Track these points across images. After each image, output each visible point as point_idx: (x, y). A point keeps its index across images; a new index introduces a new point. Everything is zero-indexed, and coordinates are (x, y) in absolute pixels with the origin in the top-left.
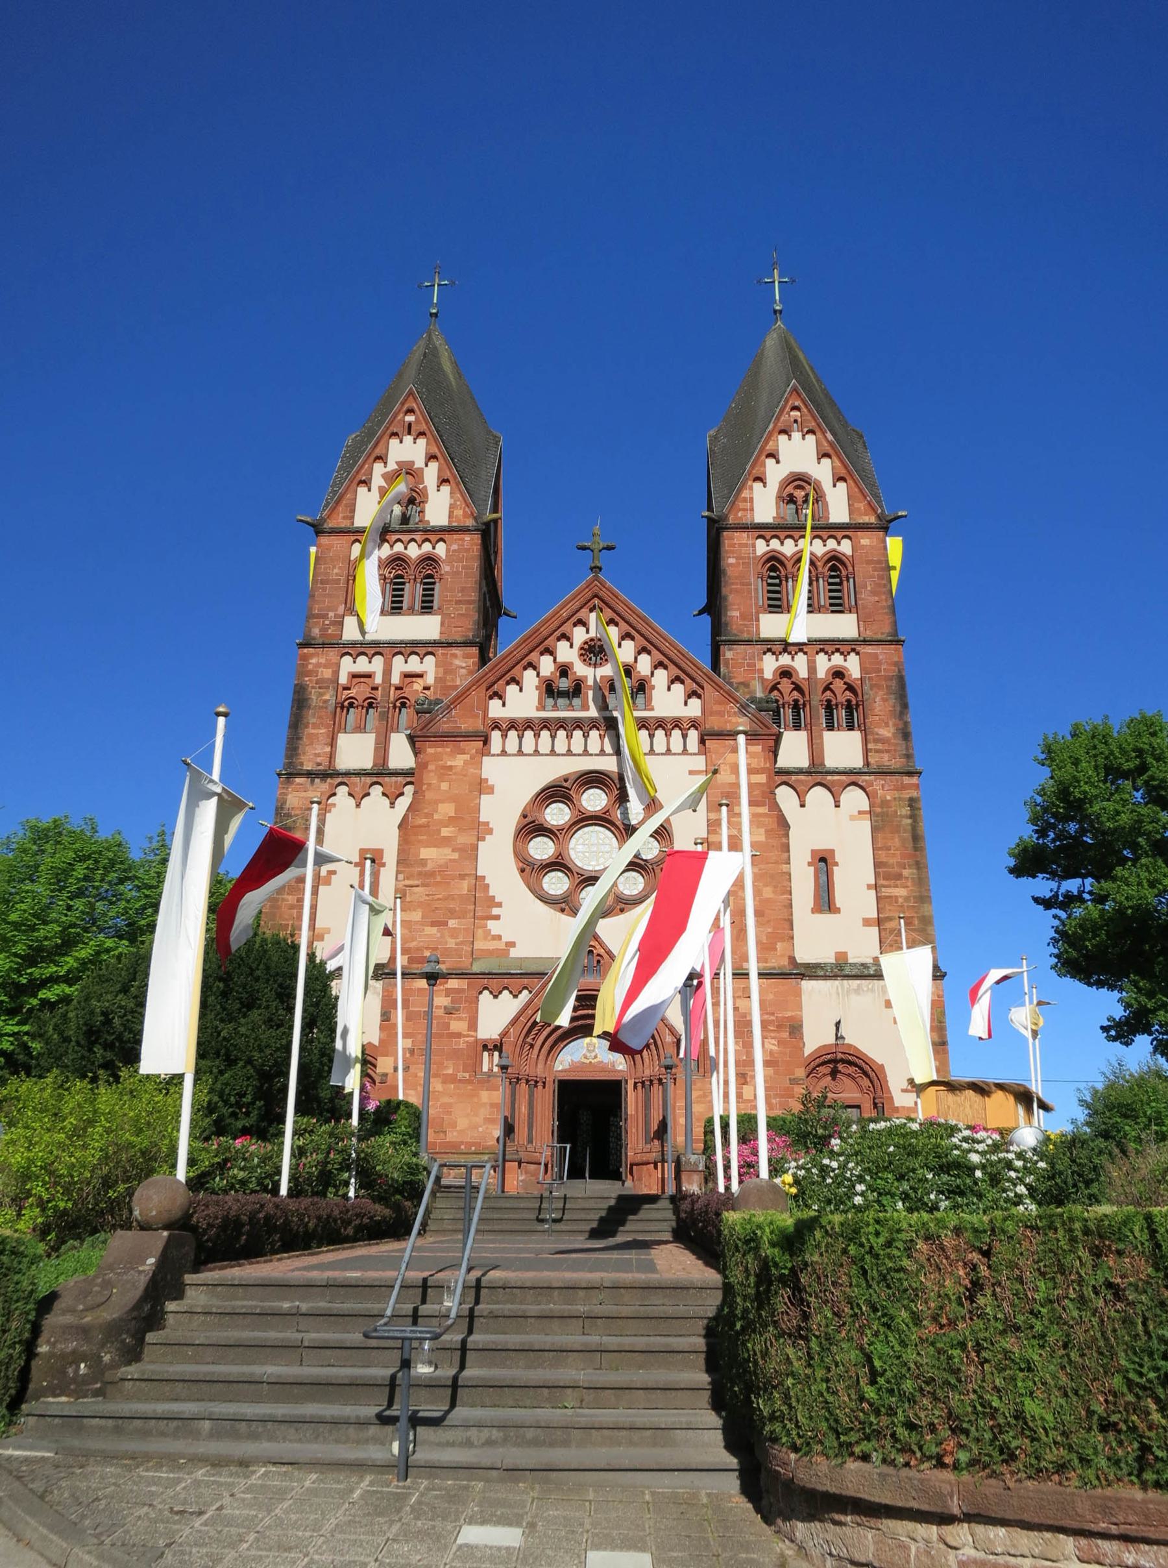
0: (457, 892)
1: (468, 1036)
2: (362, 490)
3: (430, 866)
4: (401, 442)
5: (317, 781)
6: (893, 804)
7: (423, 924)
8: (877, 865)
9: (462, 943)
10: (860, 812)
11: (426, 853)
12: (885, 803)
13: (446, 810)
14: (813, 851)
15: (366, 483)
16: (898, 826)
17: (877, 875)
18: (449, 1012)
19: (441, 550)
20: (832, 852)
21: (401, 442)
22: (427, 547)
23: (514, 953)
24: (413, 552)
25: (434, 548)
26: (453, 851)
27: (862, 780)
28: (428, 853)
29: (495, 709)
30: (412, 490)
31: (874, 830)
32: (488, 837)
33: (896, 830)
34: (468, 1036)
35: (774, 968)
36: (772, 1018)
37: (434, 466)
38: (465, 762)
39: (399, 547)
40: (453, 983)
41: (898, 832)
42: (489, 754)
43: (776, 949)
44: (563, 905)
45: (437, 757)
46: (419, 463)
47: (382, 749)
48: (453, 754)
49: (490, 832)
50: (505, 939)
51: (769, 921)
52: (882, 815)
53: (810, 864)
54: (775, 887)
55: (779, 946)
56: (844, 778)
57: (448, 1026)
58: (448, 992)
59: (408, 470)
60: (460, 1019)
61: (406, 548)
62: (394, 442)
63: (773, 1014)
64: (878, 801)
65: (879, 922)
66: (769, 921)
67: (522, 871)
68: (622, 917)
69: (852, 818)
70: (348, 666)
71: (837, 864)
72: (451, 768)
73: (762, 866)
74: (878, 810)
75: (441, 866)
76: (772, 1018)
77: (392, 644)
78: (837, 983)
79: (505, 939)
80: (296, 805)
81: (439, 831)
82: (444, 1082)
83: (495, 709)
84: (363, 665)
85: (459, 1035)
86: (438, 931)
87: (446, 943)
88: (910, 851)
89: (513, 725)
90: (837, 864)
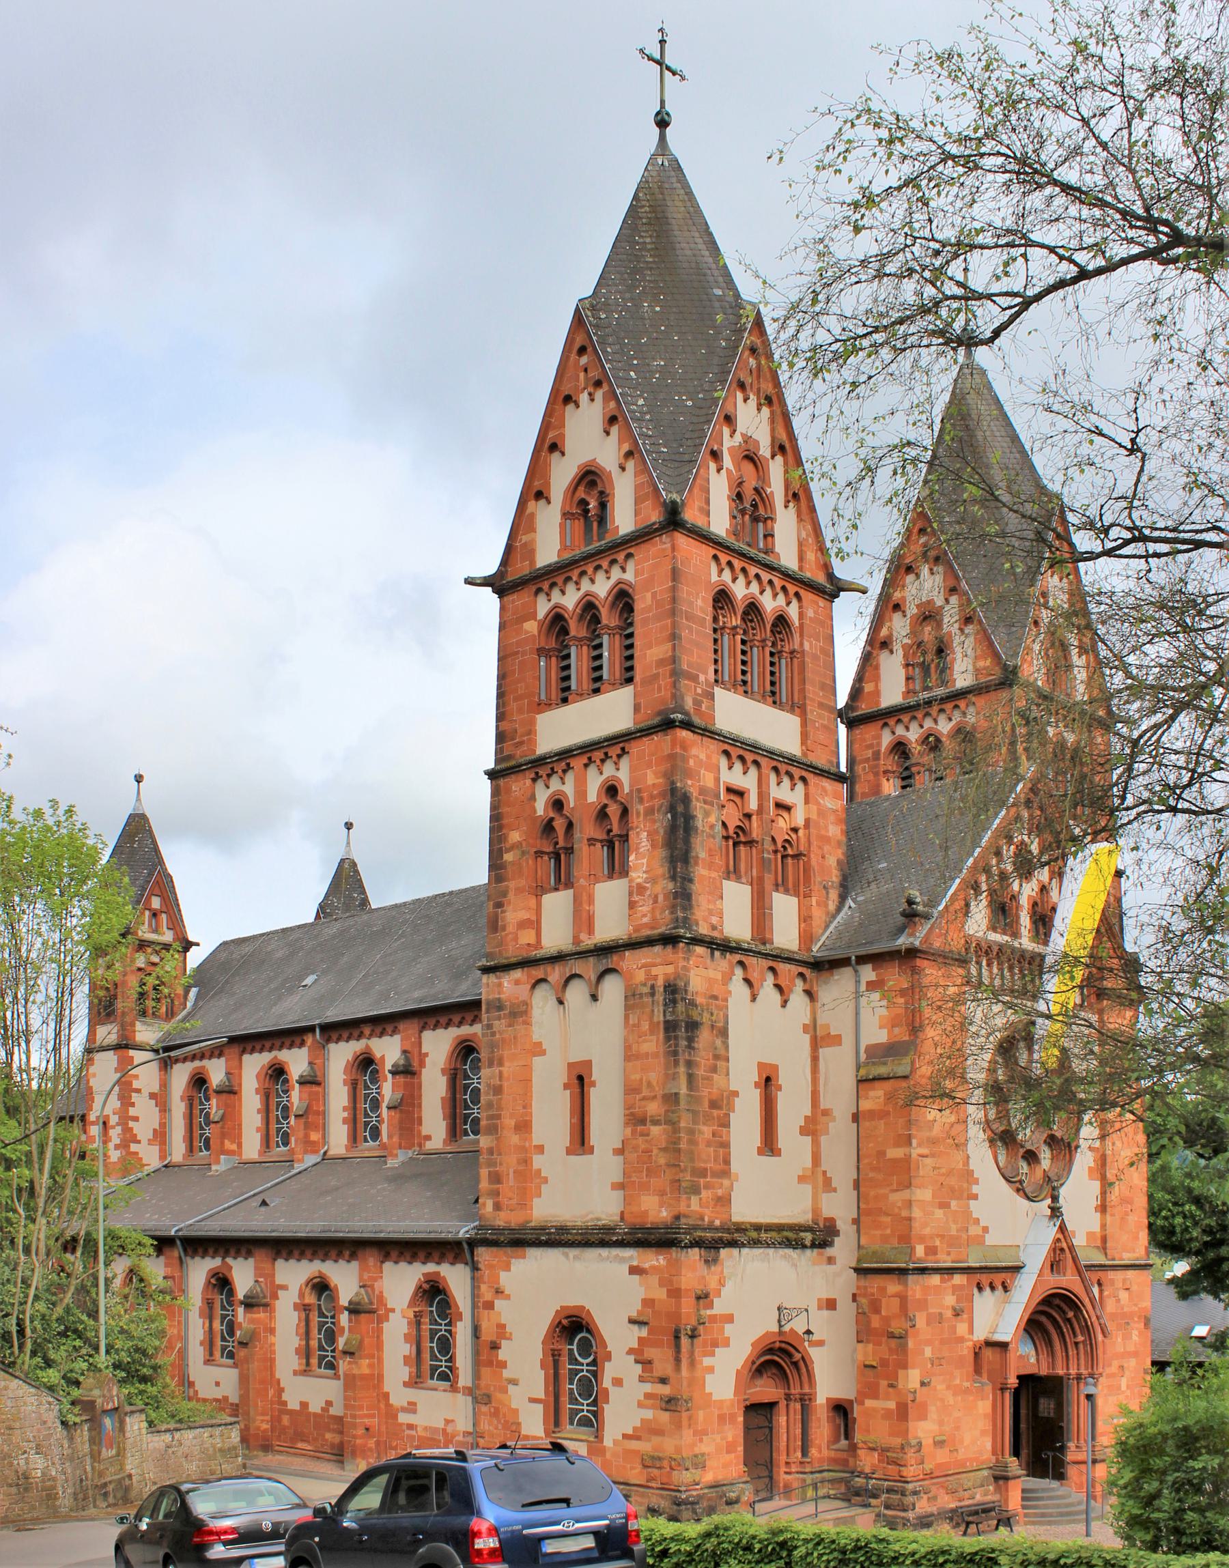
5: (717, 954)
23: (990, 1240)
50: (982, 1224)
79: (982, 1224)
82: (955, 1394)
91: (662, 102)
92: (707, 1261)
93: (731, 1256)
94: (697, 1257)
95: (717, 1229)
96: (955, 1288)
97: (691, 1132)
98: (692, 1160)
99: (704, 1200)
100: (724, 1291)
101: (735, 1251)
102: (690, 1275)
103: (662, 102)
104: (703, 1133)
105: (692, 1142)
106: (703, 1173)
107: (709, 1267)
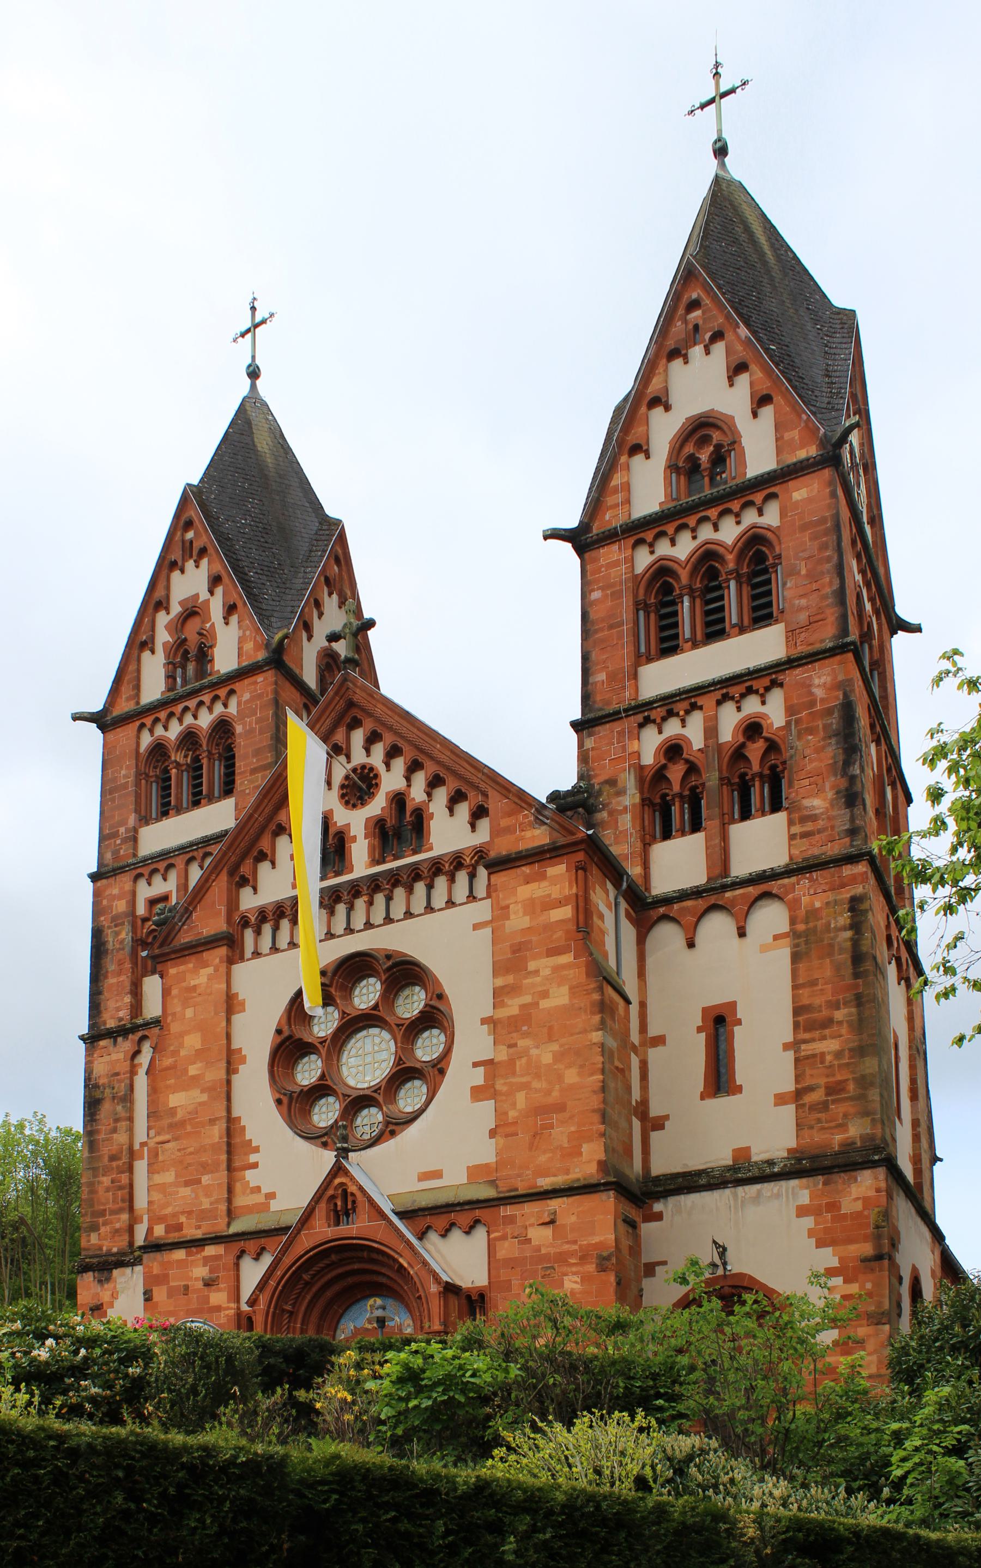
0: (207, 1141)
1: (228, 1308)
3: (180, 1115)
6: (824, 913)
7: (176, 1184)
8: (798, 1010)
9: (217, 1201)
10: (776, 938)
11: (177, 1100)
12: (813, 914)
13: (193, 1042)
14: (704, 1010)
16: (831, 946)
17: (796, 1026)
18: (209, 1284)
20: (733, 1005)
26: (202, 1091)
27: (774, 887)
28: (177, 1100)
29: (249, 901)
31: (796, 958)
32: (241, 1067)
33: (829, 950)
34: (228, 1308)
35: (578, 1180)
36: (575, 1247)
38: (210, 978)
40: (210, 1250)
41: (830, 954)
42: (242, 959)
43: (580, 1154)
44: (324, 1140)
45: (181, 978)
48: (195, 971)
49: (243, 1060)
51: (571, 1117)
52: (807, 934)
53: (699, 1030)
54: (581, 1066)
55: (585, 1148)
56: (750, 889)
57: (207, 1299)
58: (206, 1260)
60: (219, 1290)
63: (575, 1242)
64: (802, 913)
65: (798, 1095)
66: (571, 1117)
67: (279, 1102)
68: (392, 1142)
69: (764, 949)
71: (739, 1022)
72: (194, 988)
73: (563, 1040)
74: (801, 927)
75: (189, 1113)
76: (575, 1247)
77: (182, 849)
78: (727, 1192)
80: (102, 1073)
81: (186, 1071)
83: (249, 901)
85: (218, 1309)
86: (193, 1191)
87: (201, 1203)
88: (849, 980)
89: (262, 915)
90: (739, 1022)
91: (253, 357)
92: (100, 1281)
93: (124, 1274)
94: (92, 1279)
95: (114, 1255)
96: (206, 1260)
97: (91, 1184)
98: (92, 1206)
99: (102, 1234)
100: (116, 1303)
101: (128, 1270)
102: (85, 1293)
103: (253, 357)
104: (103, 1183)
105: (93, 1192)
106: (102, 1213)
107: (102, 1285)
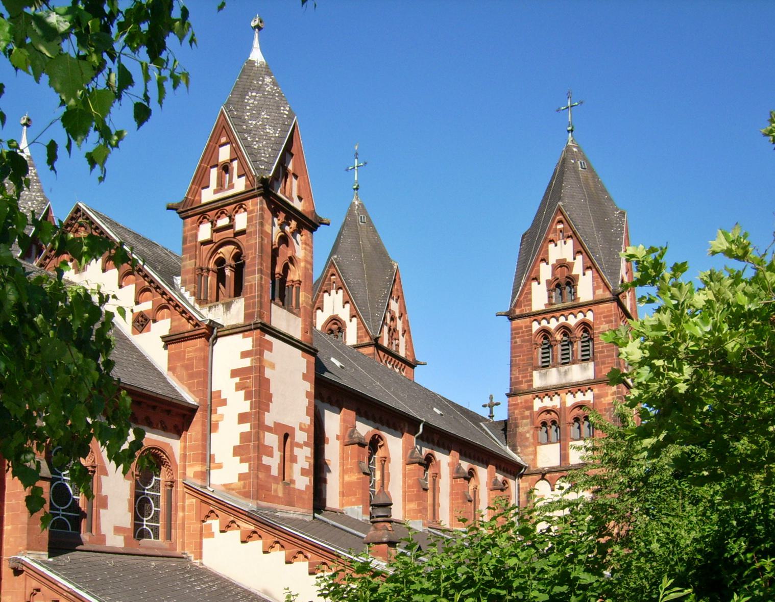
2: (534, 284)
4: (556, 245)
15: (536, 279)
19: (590, 316)
21: (556, 245)
22: (580, 316)
24: (572, 321)
25: (585, 316)
30: (567, 277)
37: (579, 258)
39: (562, 320)
46: (570, 259)
47: (564, 457)
59: (563, 265)
61: (567, 320)
62: (551, 246)
70: (537, 404)
84: (547, 403)
